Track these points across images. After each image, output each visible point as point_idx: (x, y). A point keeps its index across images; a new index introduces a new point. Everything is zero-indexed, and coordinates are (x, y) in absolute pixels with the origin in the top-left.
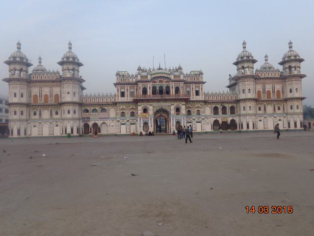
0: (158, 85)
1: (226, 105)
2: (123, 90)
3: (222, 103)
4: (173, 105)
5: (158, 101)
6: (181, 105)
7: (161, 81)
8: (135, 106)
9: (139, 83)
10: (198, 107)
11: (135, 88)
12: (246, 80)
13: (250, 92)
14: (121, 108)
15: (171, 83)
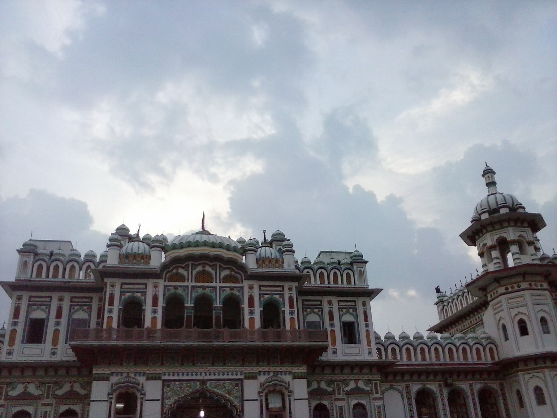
0: (190, 289)
1: (464, 386)
2: (38, 314)
3: (447, 374)
4: (253, 377)
5: (189, 356)
6: (288, 378)
7: (204, 276)
8: (83, 387)
9: (108, 281)
10: (357, 391)
11: (95, 306)
12: (524, 285)
13: (546, 331)
14: (20, 389)
15: (246, 284)
